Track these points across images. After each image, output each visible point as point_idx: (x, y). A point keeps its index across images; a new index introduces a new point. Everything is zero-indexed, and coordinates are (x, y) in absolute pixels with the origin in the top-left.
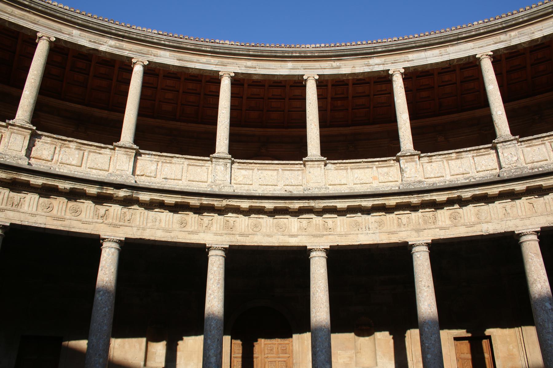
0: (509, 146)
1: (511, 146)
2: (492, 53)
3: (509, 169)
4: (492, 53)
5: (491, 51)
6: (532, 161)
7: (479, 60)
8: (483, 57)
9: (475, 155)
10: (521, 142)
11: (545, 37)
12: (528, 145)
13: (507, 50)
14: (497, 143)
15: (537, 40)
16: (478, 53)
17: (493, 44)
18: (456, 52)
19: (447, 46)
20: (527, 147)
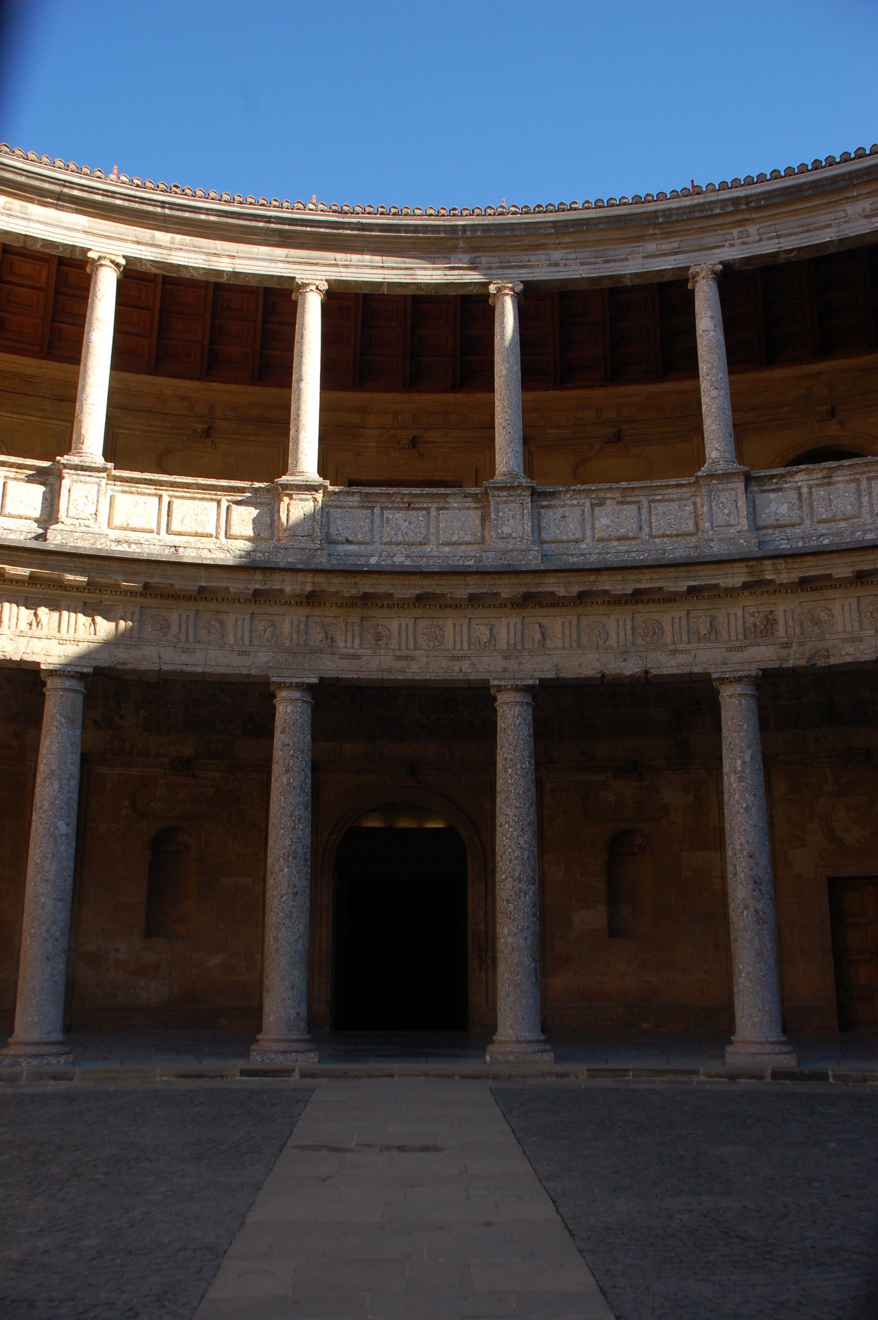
0: (88, 479)
1: (92, 479)
2: (123, 262)
3: (72, 528)
4: (123, 262)
5: (124, 257)
6: (124, 525)
7: (96, 264)
8: (103, 262)
9: (12, 475)
10: (116, 479)
11: (235, 274)
12: (127, 489)
13: (158, 268)
14: (65, 466)
15: (220, 273)
16: (96, 248)
17: (133, 242)
18: (46, 224)
19: (31, 201)
20: (123, 492)
